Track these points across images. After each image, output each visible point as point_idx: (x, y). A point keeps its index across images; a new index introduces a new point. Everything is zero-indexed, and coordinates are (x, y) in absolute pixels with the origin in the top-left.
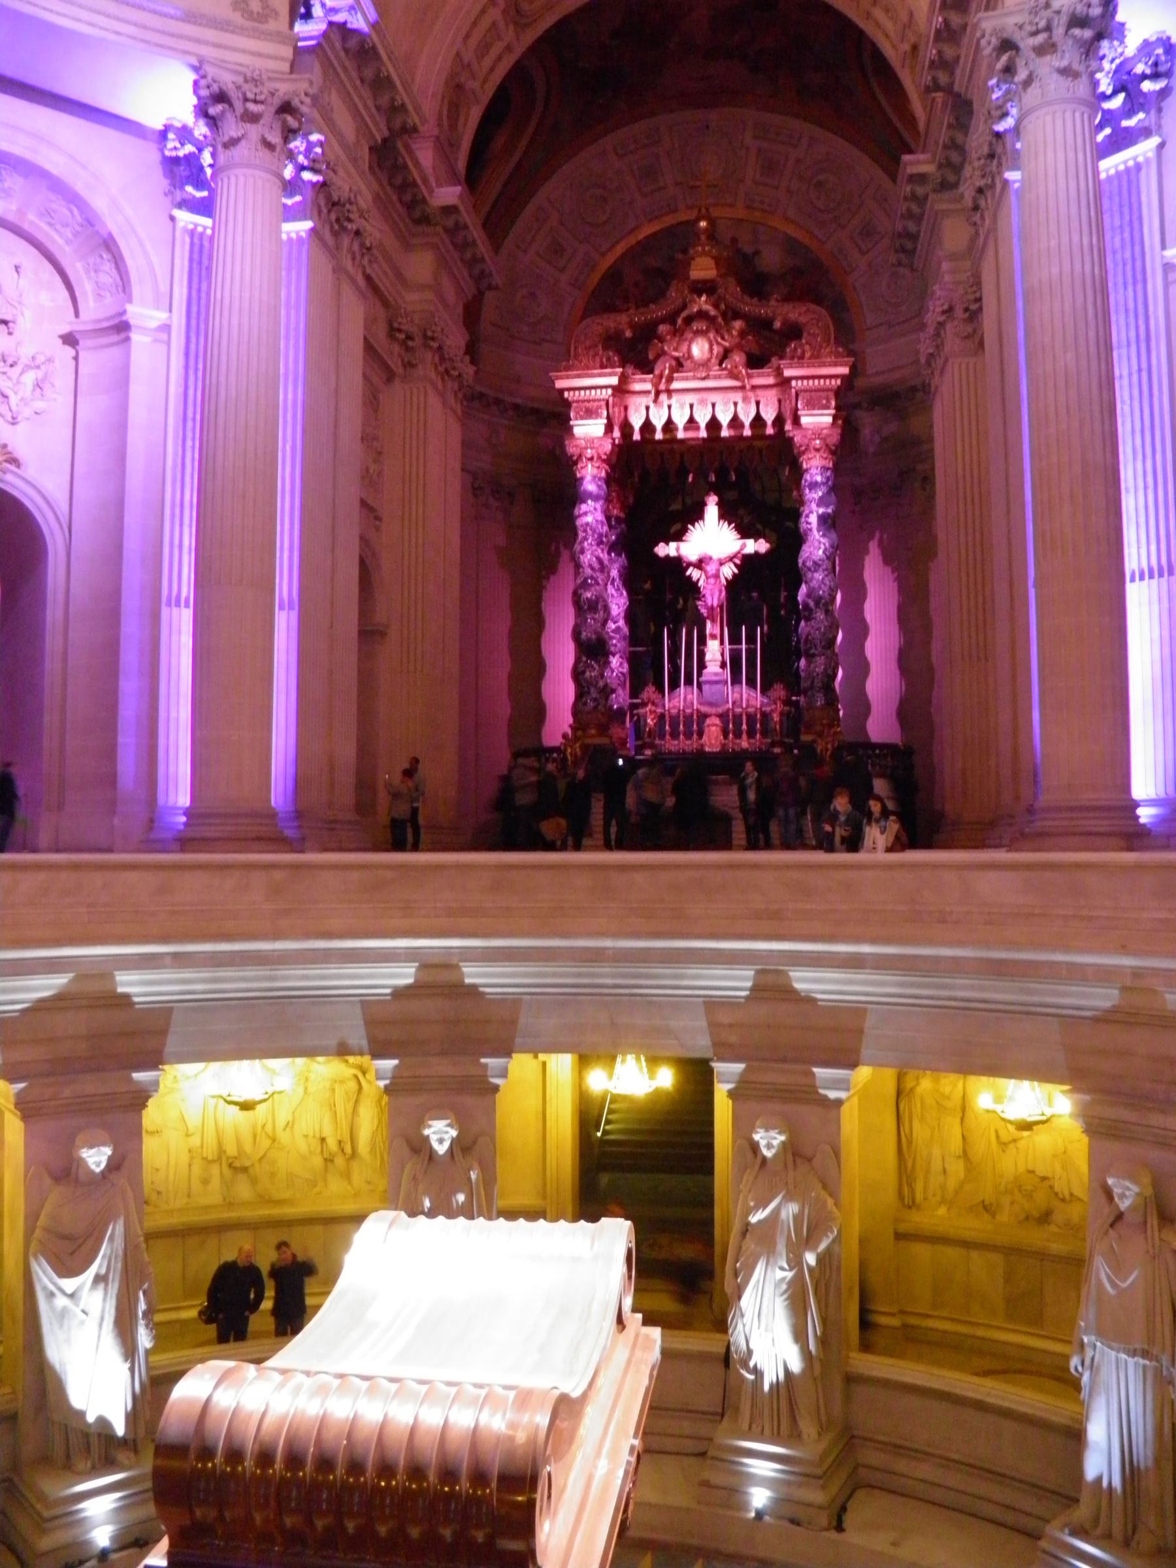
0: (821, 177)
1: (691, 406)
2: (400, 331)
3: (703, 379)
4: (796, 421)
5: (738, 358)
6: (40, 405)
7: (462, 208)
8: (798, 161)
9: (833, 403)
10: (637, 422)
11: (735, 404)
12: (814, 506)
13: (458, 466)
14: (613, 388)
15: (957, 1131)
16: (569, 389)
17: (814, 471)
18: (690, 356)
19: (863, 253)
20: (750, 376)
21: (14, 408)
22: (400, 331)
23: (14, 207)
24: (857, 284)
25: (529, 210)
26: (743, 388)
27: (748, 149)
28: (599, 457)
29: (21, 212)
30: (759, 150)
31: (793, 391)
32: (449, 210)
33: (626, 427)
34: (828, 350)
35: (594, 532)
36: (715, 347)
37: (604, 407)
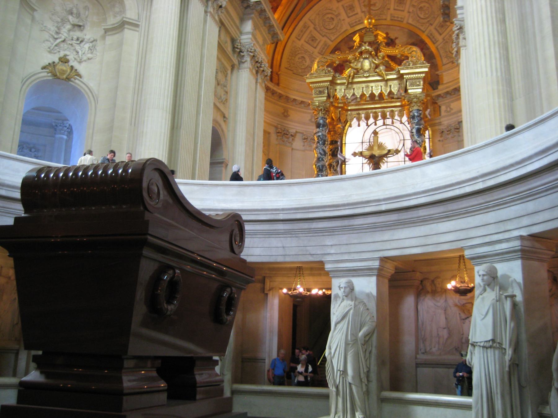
0: (422, 5)
1: (363, 88)
2: (237, 48)
4: (406, 91)
6: (90, 56)
9: (422, 83)
10: (339, 95)
11: (381, 86)
12: (414, 125)
13: (263, 107)
14: (330, 81)
15: (443, 317)
17: (414, 111)
18: (362, 68)
19: (441, 34)
20: (387, 75)
21: (80, 56)
22: (237, 48)
25: (301, 24)
26: (383, 80)
28: (324, 110)
31: (405, 80)
35: (322, 139)
36: (372, 64)
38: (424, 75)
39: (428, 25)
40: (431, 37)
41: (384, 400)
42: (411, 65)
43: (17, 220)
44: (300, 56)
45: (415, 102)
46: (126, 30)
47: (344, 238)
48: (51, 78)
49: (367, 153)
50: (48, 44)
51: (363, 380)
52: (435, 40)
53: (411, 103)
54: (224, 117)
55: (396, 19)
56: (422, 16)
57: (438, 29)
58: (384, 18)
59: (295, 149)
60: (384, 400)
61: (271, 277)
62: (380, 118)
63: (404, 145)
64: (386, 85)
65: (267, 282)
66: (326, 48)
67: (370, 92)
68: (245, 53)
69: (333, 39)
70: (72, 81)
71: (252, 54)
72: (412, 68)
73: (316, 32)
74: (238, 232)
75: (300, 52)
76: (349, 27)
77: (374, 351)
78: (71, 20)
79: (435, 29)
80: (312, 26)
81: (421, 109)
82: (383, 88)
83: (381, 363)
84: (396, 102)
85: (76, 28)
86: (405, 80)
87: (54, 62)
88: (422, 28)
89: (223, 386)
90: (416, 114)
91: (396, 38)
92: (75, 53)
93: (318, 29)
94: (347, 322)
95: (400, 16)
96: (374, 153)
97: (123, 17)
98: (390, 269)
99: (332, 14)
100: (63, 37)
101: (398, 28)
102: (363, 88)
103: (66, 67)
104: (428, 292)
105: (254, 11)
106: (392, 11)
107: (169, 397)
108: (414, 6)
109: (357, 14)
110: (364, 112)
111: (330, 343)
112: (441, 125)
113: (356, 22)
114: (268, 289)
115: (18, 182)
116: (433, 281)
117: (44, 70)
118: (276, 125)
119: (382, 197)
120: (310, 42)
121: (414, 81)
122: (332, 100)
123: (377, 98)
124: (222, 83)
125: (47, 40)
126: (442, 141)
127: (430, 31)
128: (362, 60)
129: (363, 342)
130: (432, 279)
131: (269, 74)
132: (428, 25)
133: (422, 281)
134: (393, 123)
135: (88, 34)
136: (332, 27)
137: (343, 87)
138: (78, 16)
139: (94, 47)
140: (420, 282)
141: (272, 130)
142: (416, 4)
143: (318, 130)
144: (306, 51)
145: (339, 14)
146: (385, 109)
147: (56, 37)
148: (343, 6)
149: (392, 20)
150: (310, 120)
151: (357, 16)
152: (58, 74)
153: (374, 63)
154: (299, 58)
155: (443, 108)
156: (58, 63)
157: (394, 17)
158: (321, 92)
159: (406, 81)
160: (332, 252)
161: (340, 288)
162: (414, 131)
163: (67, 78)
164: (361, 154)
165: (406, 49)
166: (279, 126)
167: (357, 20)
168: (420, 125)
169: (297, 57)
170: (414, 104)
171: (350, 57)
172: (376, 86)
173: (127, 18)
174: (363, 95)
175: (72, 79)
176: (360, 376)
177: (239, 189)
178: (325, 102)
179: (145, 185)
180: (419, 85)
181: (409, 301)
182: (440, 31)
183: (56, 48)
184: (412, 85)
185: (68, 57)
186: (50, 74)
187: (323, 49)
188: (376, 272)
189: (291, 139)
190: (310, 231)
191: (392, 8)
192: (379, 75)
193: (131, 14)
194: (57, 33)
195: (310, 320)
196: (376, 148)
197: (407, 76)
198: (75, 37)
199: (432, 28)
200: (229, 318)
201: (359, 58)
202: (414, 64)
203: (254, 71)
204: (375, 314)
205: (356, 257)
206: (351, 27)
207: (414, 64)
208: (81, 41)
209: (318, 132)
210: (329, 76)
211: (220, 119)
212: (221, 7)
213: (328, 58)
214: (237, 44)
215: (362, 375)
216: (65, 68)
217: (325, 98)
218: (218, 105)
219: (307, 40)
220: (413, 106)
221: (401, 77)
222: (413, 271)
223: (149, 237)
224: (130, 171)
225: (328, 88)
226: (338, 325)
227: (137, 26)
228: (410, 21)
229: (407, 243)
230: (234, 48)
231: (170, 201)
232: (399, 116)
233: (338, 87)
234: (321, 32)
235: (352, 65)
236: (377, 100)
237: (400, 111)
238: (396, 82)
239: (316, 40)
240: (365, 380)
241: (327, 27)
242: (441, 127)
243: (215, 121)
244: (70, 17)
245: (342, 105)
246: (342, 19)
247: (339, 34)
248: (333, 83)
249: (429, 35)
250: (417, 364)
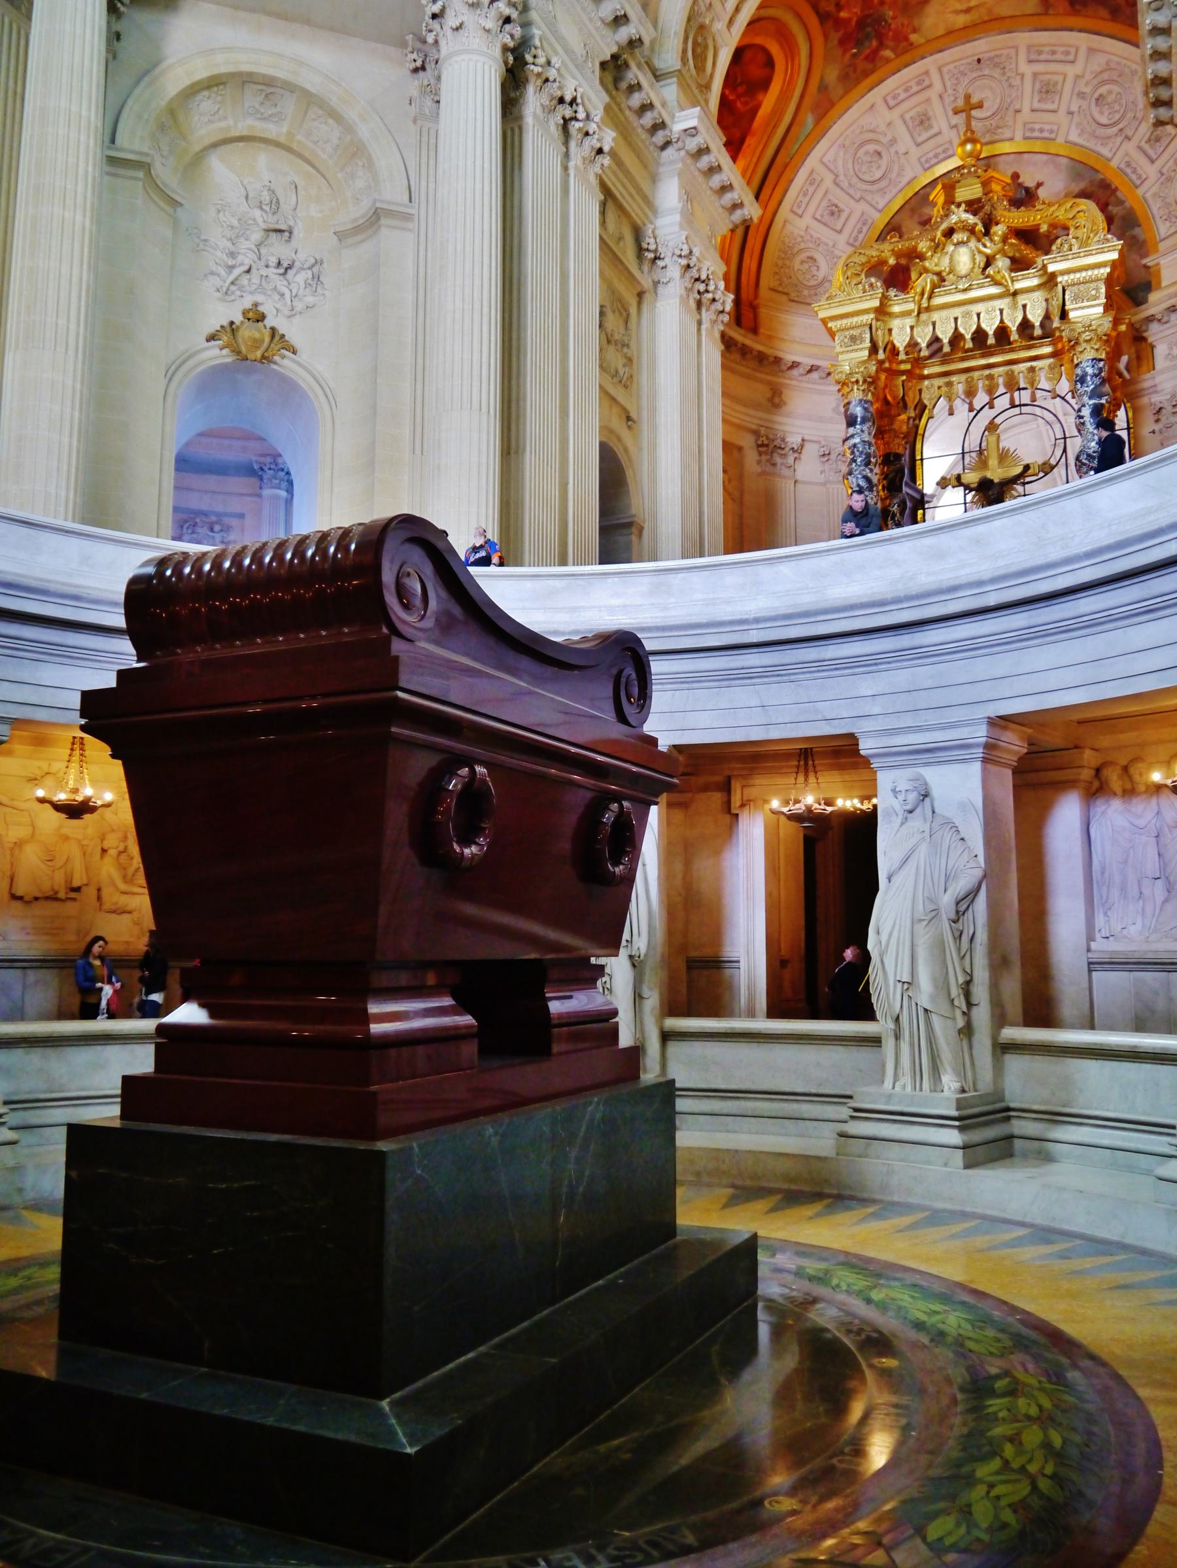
0: (1103, 90)
1: (956, 319)
2: (648, 250)
3: (965, 290)
4: (1064, 315)
5: (1002, 263)
6: (310, 300)
7: (701, 129)
8: (1078, 77)
9: (1103, 290)
10: (900, 342)
12: (1085, 398)
13: (718, 389)
15: (1152, 852)
16: (834, 318)
19: (1152, 161)
22: (648, 250)
23: (285, 130)
24: (1148, 195)
27: (1023, 76)
28: (865, 381)
29: (290, 134)
30: (1035, 75)
31: (1060, 287)
32: (691, 132)
33: (894, 352)
34: (1096, 239)
36: (977, 257)
37: (868, 331)
38: (1108, 270)
39: (1119, 139)
40: (1129, 171)
41: (1004, 1048)
42: (1075, 250)
43: (123, 675)
44: (804, 256)
45: (1086, 341)
46: (384, 230)
47: (901, 677)
48: (229, 360)
49: (972, 478)
50: (217, 281)
51: (956, 1003)
52: (1139, 177)
53: (1077, 343)
54: (629, 418)
55: (1036, 134)
56: (1104, 121)
57: (1146, 147)
58: (1008, 135)
59: (805, 483)
60: (1004, 1048)
61: (744, 777)
62: (1002, 390)
63: (1065, 451)
64: (1014, 306)
65: (736, 786)
66: (865, 229)
67: (974, 327)
68: (667, 261)
69: (880, 206)
70: (275, 363)
71: (684, 262)
72: (1077, 256)
73: (838, 192)
74: (634, 676)
75: (803, 246)
76: (919, 169)
77: (982, 936)
78: (260, 220)
79: (1140, 148)
80: (829, 178)
81: (1103, 356)
82: (1005, 312)
83: (999, 963)
84: (1042, 345)
85: (273, 235)
86: (1060, 287)
87: (232, 323)
88: (1106, 152)
89: (617, 1023)
90: (1090, 371)
91: (1039, 185)
92: (277, 297)
93: (845, 185)
94: (914, 871)
95: (1047, 127)
96: (989, 475)
97: (375, 201)
98: (1014, 744)
99: (877, 142)
100: (247, 262)
101: (1045, 157)
102: (956, 319)
103: (259, 331)
104: (1115, 794)
105: (683, 153)
106: (1026, 114)
107: (482, 1051)
108: (1081, 95)
109: (939, 133)
110: (963, 377)
111: (878, 921)
112: (1156, 392)
113: (936, 156)
114: (738, 804)
115: (118, 590)
116: (1125, 769)
117: (213, 343)
118: (754, 427)
119: (987, 576)
120: (827, 218)
121: (1082, 287)
122: (881, 355)
123: (991, 341)
124: (616, 337)
125: (212, 273)
126: (1161, 432)
127: (1127, 154)
128: (952, 248)
129: (953, 916)
130: (1124, 762)
131: (729, 306)
132: (1119, 139)
133: (1098, 771)
134: (1034, 399)
135: (303, 248)
136: (878, 175)
137: (909, 321)
138: (275, 205)
139: (317, 278)
140: (1093, 772)
141: (747, 441)
142: (1088, 90)
143: (851, 430)
144: (818, 243)
145: (893, 141)
146: (1014, 367)
147: (231, 262)
148: (902, 116)
149: (1025, 138)
150: (835, 410)
151: (939, 139)
152: (244, 349)
153: (980, 252)
154: (802, 262)
155: (1161, 351)
156: (242, 322)
157: (1032, 130)
158: (853, 339)
159: (1064, 291)
160: (876, 710)
161: (895, 792)
162: (1086, 412)
163: (263, 357)
164: (959, 481)
165: (1063, 209)
166: (763, 431)
167: (940, 150)
168: (1100, 397)
169: (797, 260)
170: (1084, 345)
171: (923, 246)
172: (987, 312)
173: (382, 201)
174: (957, 338)
175: (277, 358)
176: (949, 994)
177: (655, 579)
178: (864, 362)
179: (388, 576)
180: (1096, 298)
181: (1067, 814)
182: (1151, 152)
183: (233, 288)
184: (1076, 299)
185: (261, 308)
186: (225, 352)
187: (860, 232)
188: (979, 752)
189: (790, 460)
190: (821, 665)
191: (1026, 109)
192: (997, 283)
193: (393, 193)
194: (232, 255)
195: (836, 869)
196: (993, 462)
197: (1066, 277)
198: (273, 261)
199: (1130, 147)
200: (619, 870)
201: (944, 245)
202: (1084, 243)
203: (693, 305)
204: (980, 850)
205: (932, 718)
206: (926, 170)
207: (1084, 243)
208: (285, 268)
209: (852, 436)
210: (872, 298)
211: (618, 425)
212: (600, 151)
213: (867, 252)
214: (649, 242)
215: (955, 991)
216: (257, 335)
217: (866, 353)
218: (612, 391)
219: (818, 216)
220: (1081, 352)
221: (1050, 281)
222: (1076, 747)
223: (400, 694)
224: (353, 547)
225: (871, 328)
226: (893, 879)
227: (407, 217)
228: (1074, 137)
229: (1054, 680)
230: (640, 251)
231: (457, 611)
232: (1049, 379)
233: (895, 324)
234: (852, 192)
235: (927, 264)
236: (991, 346)
237: (1051, 368)
238: (1039, 296)
239: (840, 211)
240: (961, 1002)
241: (867, 177)
242: (1156, 399)
243: (605, 429)
244: (257, 213)
245: (908, 366)
246: (902, 150)
247: (895, 191)
248: (882, 312)
249: (1122, 166)
250: (1090, 963)
